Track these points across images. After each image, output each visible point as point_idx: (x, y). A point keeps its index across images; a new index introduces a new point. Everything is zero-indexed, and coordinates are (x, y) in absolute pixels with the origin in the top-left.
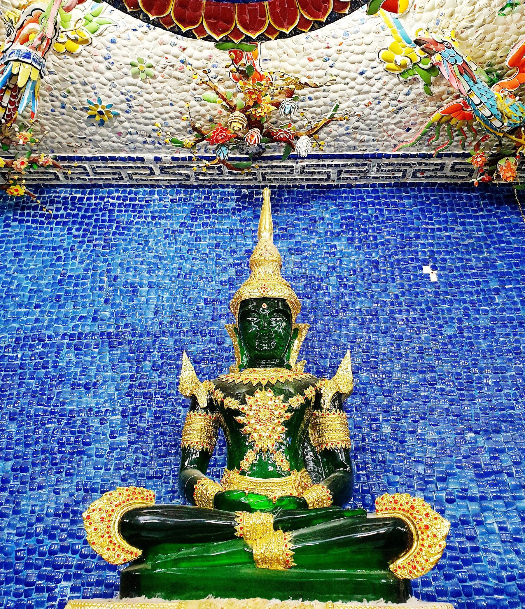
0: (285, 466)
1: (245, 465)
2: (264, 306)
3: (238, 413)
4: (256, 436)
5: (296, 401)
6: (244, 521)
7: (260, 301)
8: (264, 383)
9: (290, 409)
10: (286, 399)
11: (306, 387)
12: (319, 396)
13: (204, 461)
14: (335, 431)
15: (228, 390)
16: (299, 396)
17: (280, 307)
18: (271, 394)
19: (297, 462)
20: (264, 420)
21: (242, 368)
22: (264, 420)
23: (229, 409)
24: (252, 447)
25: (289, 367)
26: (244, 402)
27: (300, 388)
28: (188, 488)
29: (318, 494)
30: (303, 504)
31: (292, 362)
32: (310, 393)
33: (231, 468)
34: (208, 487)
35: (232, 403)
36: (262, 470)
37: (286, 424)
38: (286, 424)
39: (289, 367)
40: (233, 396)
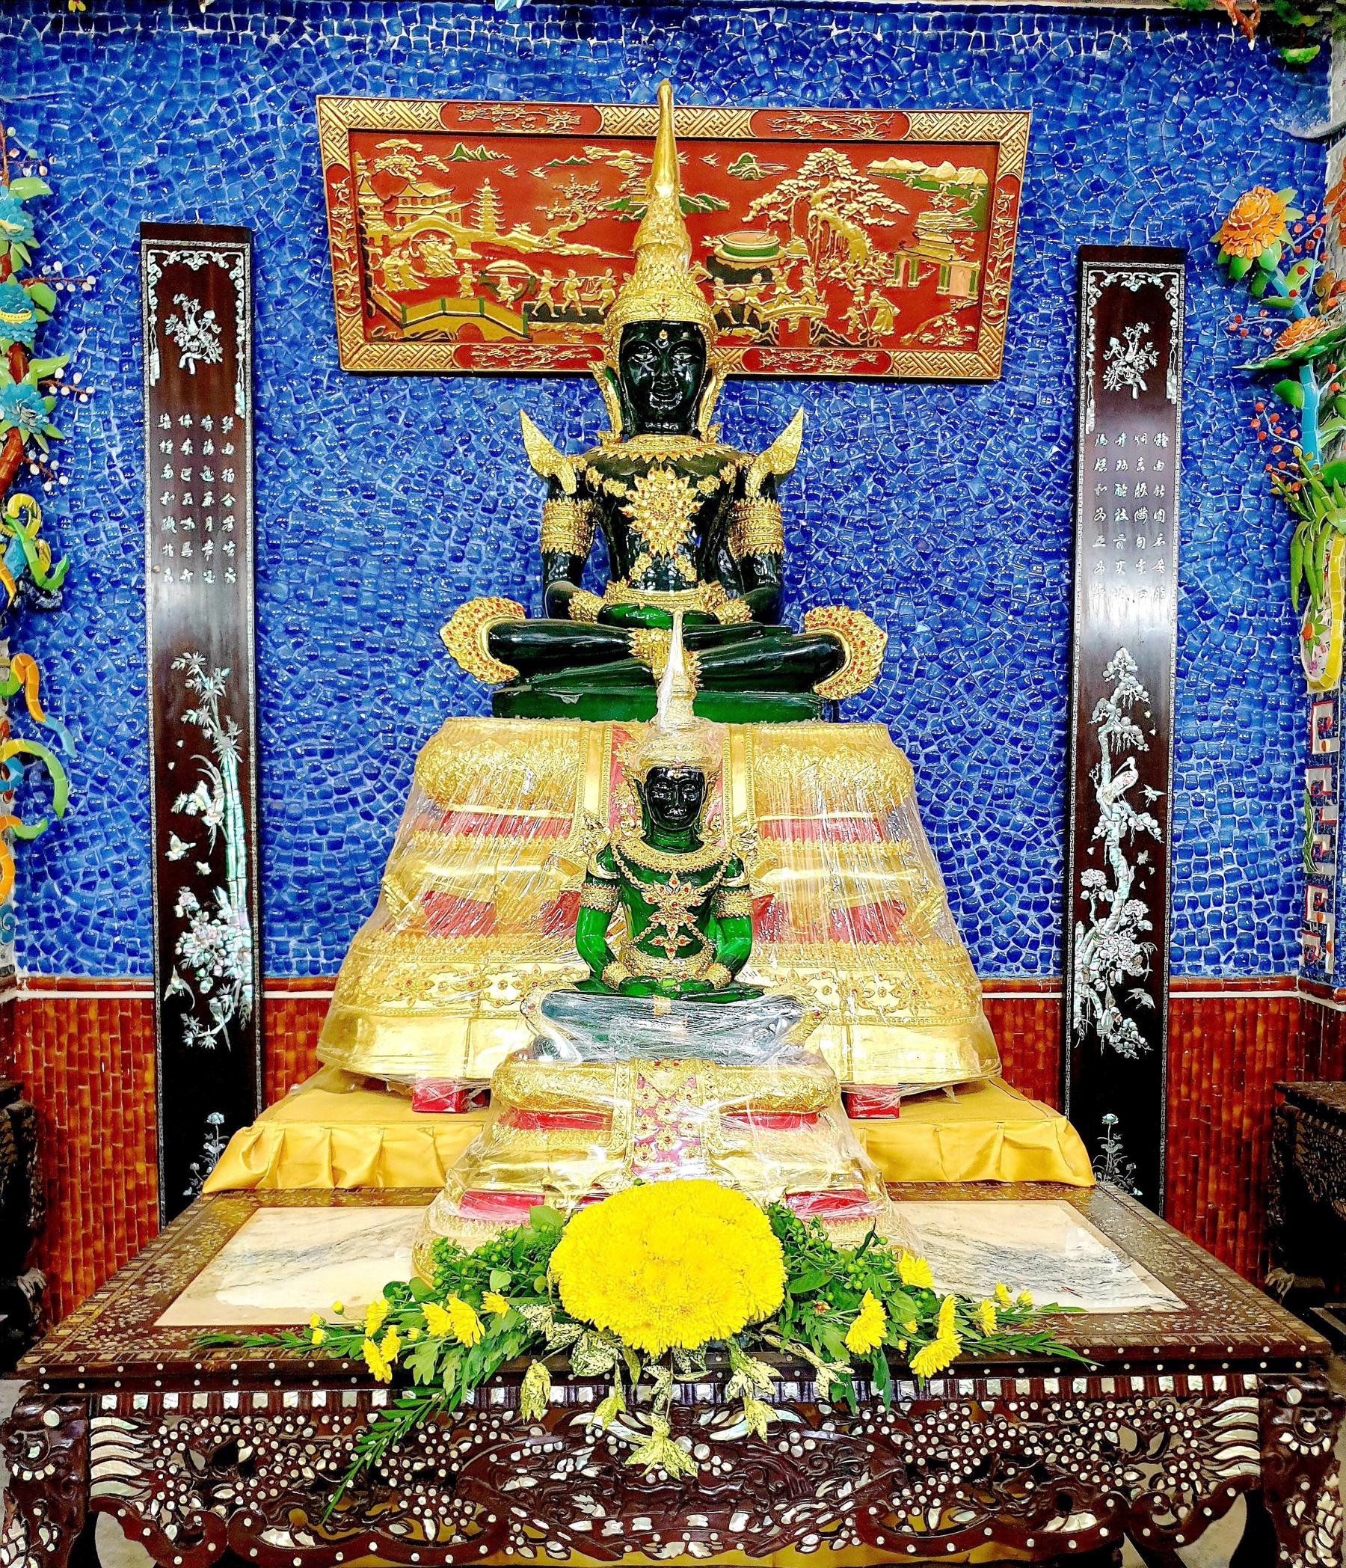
0: (691, 575)
1: (636, 572)
2: (663, 335)
3: (624, 501)
4: (650, 535)
5: (709, 486)
6: (640, 640)
7: (653, 327)
8: (661, 459)
9: (699, 498)
10: (693, 483)
11: (723, 464)
12: (741, 477)
13: (576, 570)
14: (762, 528)
15: (606, 468)
16: (710, 479)
17: (688, 339)
18: (670, 475)
19: (708, 571)
20: (662, 511)
21: (626, 435)
22: (662, 511)
23: (611, 496)
24: (646, 550)
25: (697, 434)
26: (632, 486)
27: (714, 465)
28: (559, 606)
29: (734, 610)
30: (713, 620)
31: (702, 424)
32: (728, 474)
33: (616, 578)
34: (585, 603)
35: (617, 489)
36: (661, 580)
37: (693, 518)
38: (693, 518)
39: (697, 434)
40: (616, 477)
